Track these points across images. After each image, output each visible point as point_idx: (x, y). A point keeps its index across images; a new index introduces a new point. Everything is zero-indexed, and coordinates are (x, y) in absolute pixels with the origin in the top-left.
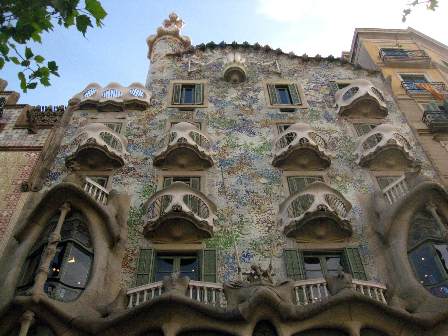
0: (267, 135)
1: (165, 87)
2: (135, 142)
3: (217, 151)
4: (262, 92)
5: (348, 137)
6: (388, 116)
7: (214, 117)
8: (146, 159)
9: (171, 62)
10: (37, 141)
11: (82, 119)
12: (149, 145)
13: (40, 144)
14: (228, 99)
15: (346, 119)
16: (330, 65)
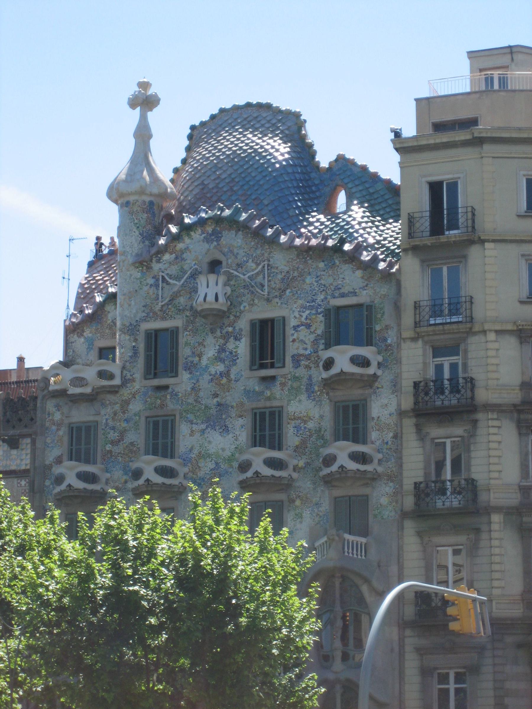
0: (239, 433)
1: (136, 340)
2: (114, 453)
3: (189, 464)
4: (243, 340)
5: (323, 430)
6: (379, 380)
7: (189, 401)
8: (126, 482)
9: (139, 275)
10: (22, 460)
11: (57, 416)
12: (127, 459)
13: (26, 465)
14: (204, 361)
15: (327, 394)
16: (337, 258)
